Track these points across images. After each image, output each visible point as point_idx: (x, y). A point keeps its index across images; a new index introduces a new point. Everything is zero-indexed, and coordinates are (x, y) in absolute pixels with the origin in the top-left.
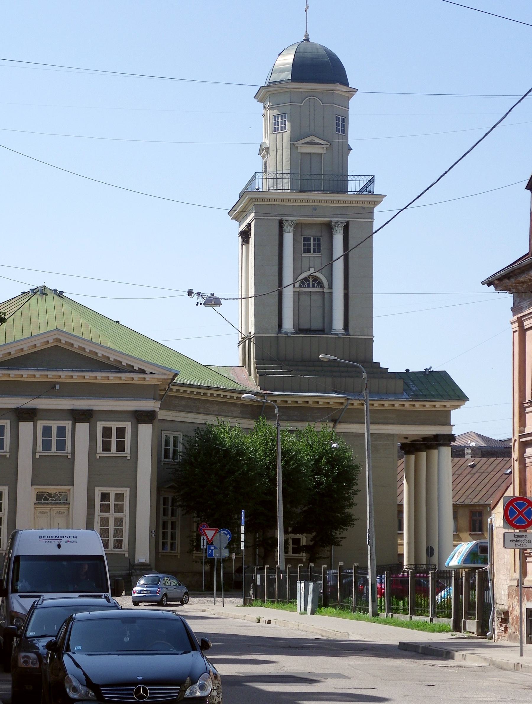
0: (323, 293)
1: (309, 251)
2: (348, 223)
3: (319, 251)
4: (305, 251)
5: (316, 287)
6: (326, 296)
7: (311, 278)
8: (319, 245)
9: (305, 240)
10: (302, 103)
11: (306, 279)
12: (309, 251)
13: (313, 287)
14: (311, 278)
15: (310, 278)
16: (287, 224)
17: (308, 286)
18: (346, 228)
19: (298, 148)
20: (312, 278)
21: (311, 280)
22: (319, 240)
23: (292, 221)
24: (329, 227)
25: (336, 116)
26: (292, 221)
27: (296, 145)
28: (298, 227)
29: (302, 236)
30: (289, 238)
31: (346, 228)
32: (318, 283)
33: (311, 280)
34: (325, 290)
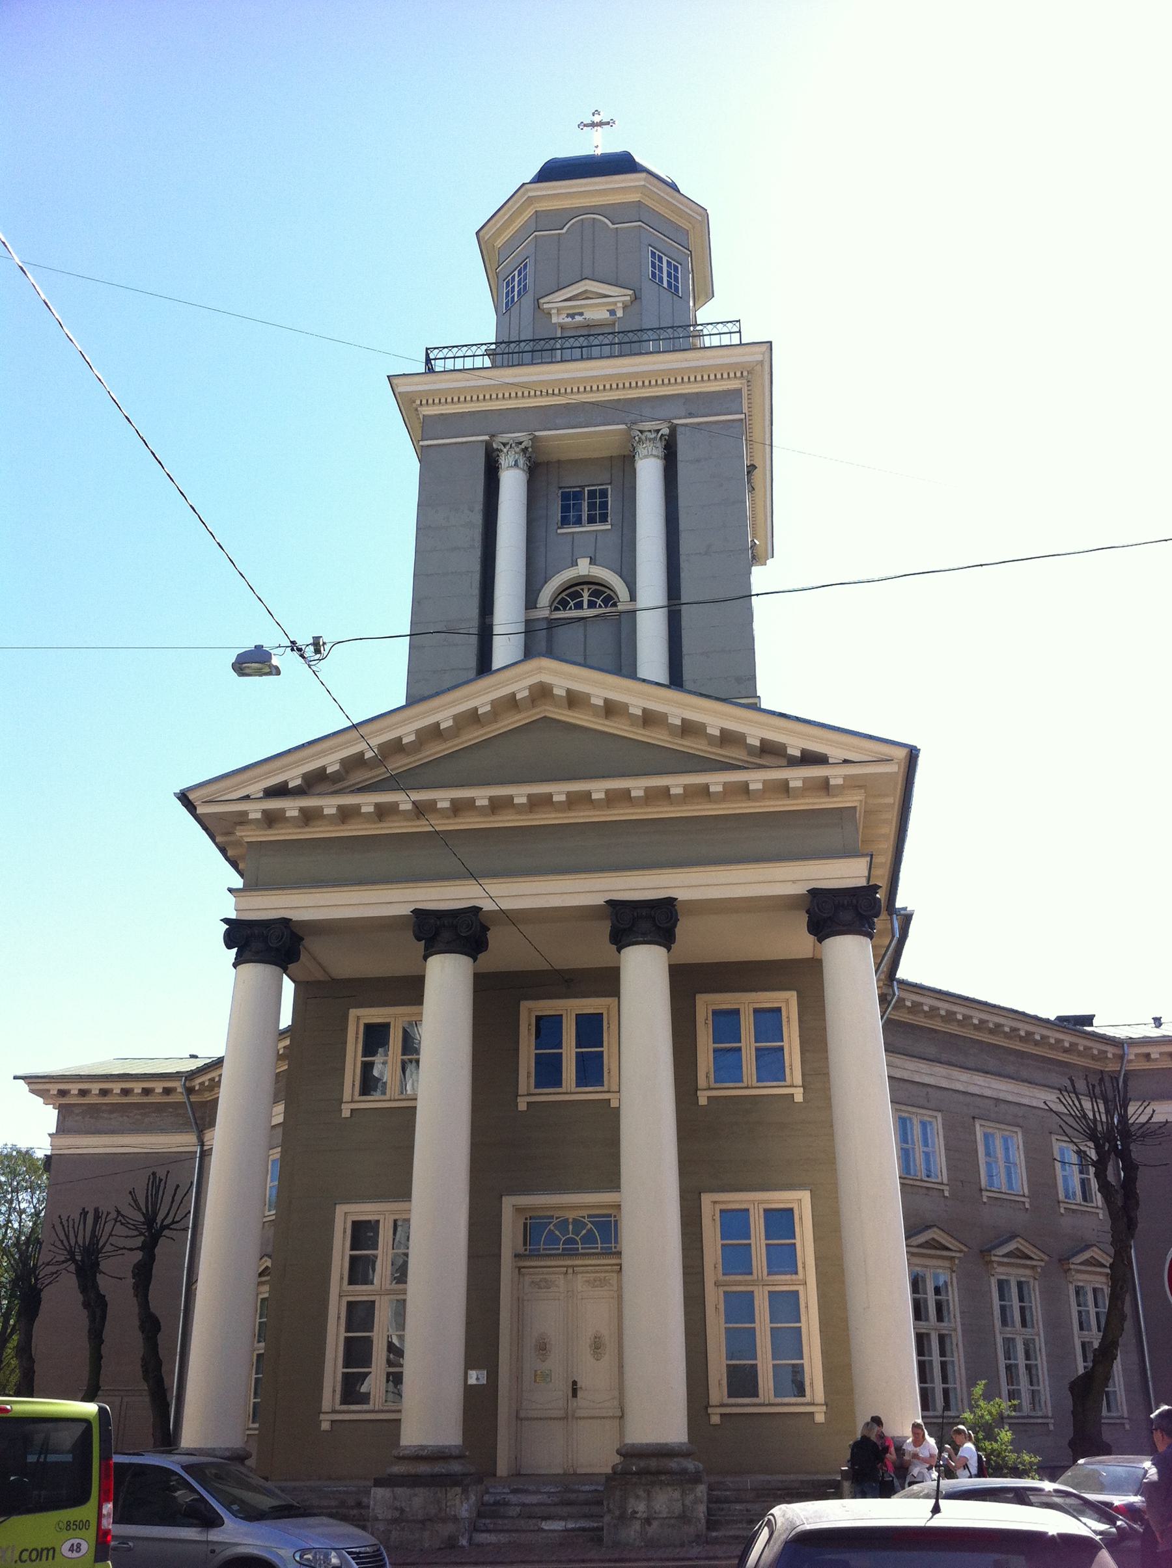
2: (673, 429)
3: (604, 519)
4: (565, 521)
5: (600, 606)
7: (586, 591)
8: (604, 505)
9: (565, 497)
10: (562, 229)
12: (579, 522)
13: (592, 605)
14: (586, 591)
15: (583, 590)
16: (505, 450)
17: (579, 606)
19: (553, 311)
20: (589, 589)
21: (586, 595)
22: (604, 494)
23: (521, 443)
25: (650, 248)
26: (521, 443)
27: (545, 306)
29: (560, 488)
32: (601, 593)
33: (586, 595)
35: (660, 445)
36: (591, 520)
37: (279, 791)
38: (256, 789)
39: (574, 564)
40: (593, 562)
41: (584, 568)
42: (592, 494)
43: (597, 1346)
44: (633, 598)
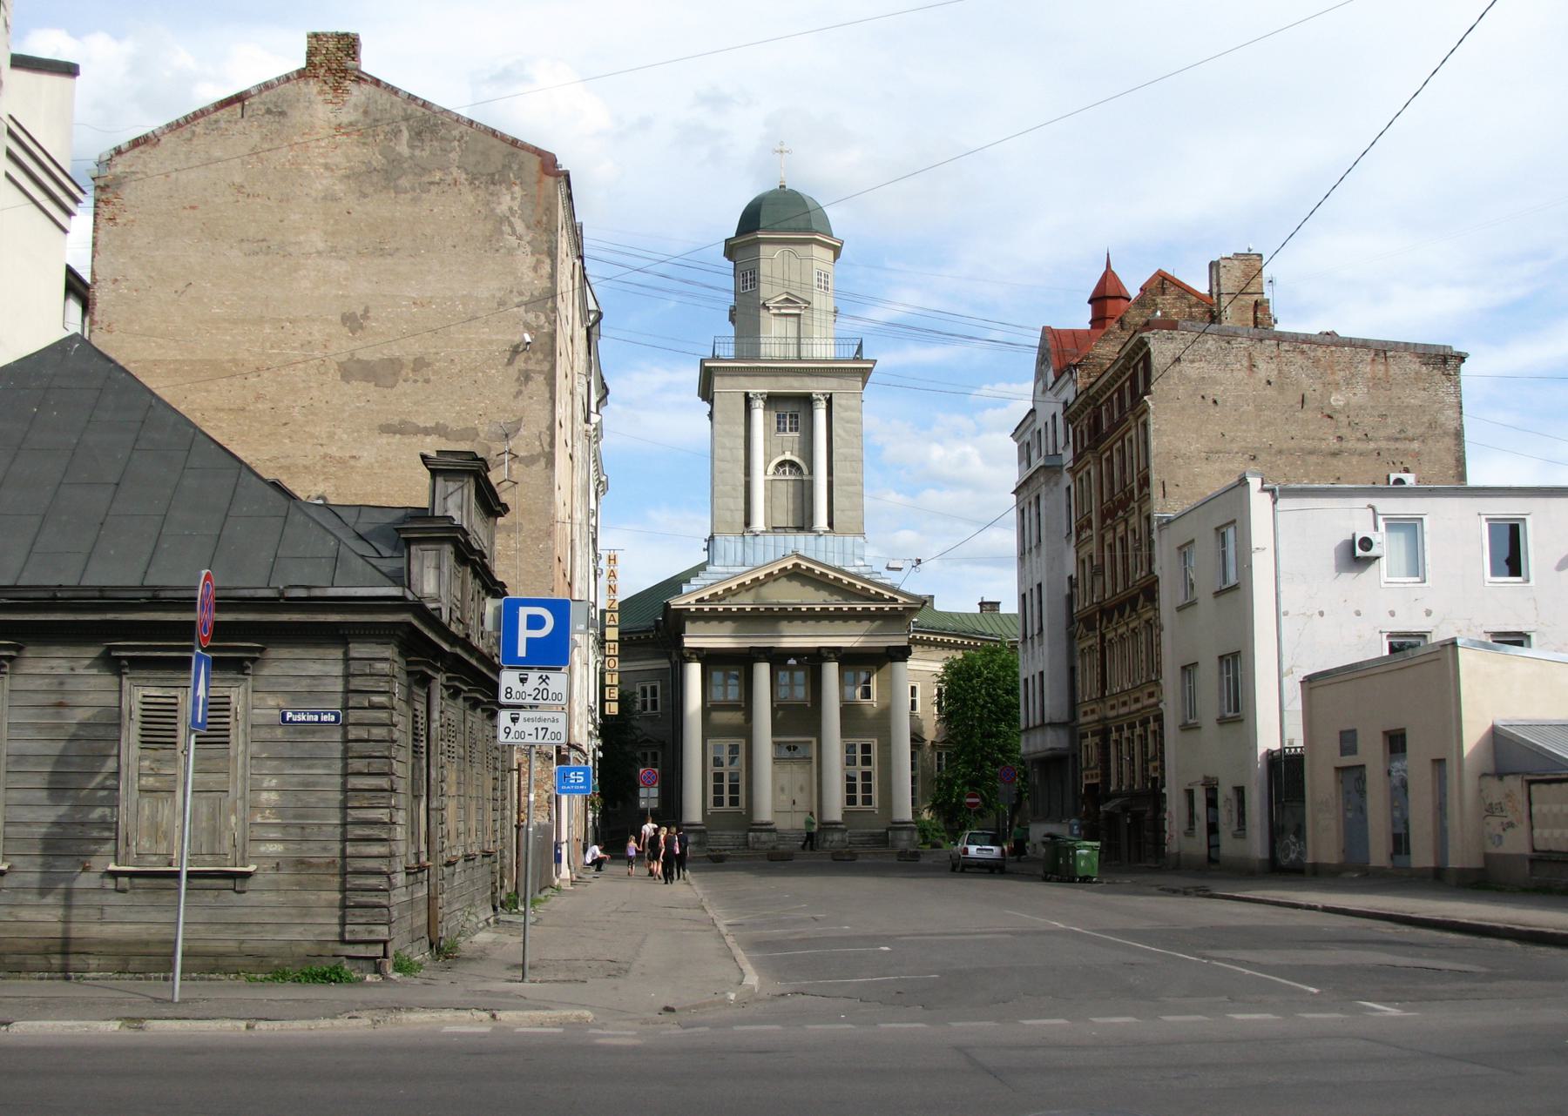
0: (802, 481)
1: (785, 430)
2: (831, 394)
3: (796, 430)
6: (806, 484)
8: (797, 423)
9: (779, 416)
11: (782, 464)
12: (785, 430)
18: (829, 402)
22: (797, 417)
24: (807, 401)
28: (772, 400)
30: (759, 414)
31: (829, 402)
34: (805, 478)
35: (824, 402)
36: (791, 430)
37: (700, 600)
38: (692, 600)
39: (784, 453)
40: (792, 454)
41: (788, 456)
42: (791, 416)
43: (801, 789)
44: (811, 472)
